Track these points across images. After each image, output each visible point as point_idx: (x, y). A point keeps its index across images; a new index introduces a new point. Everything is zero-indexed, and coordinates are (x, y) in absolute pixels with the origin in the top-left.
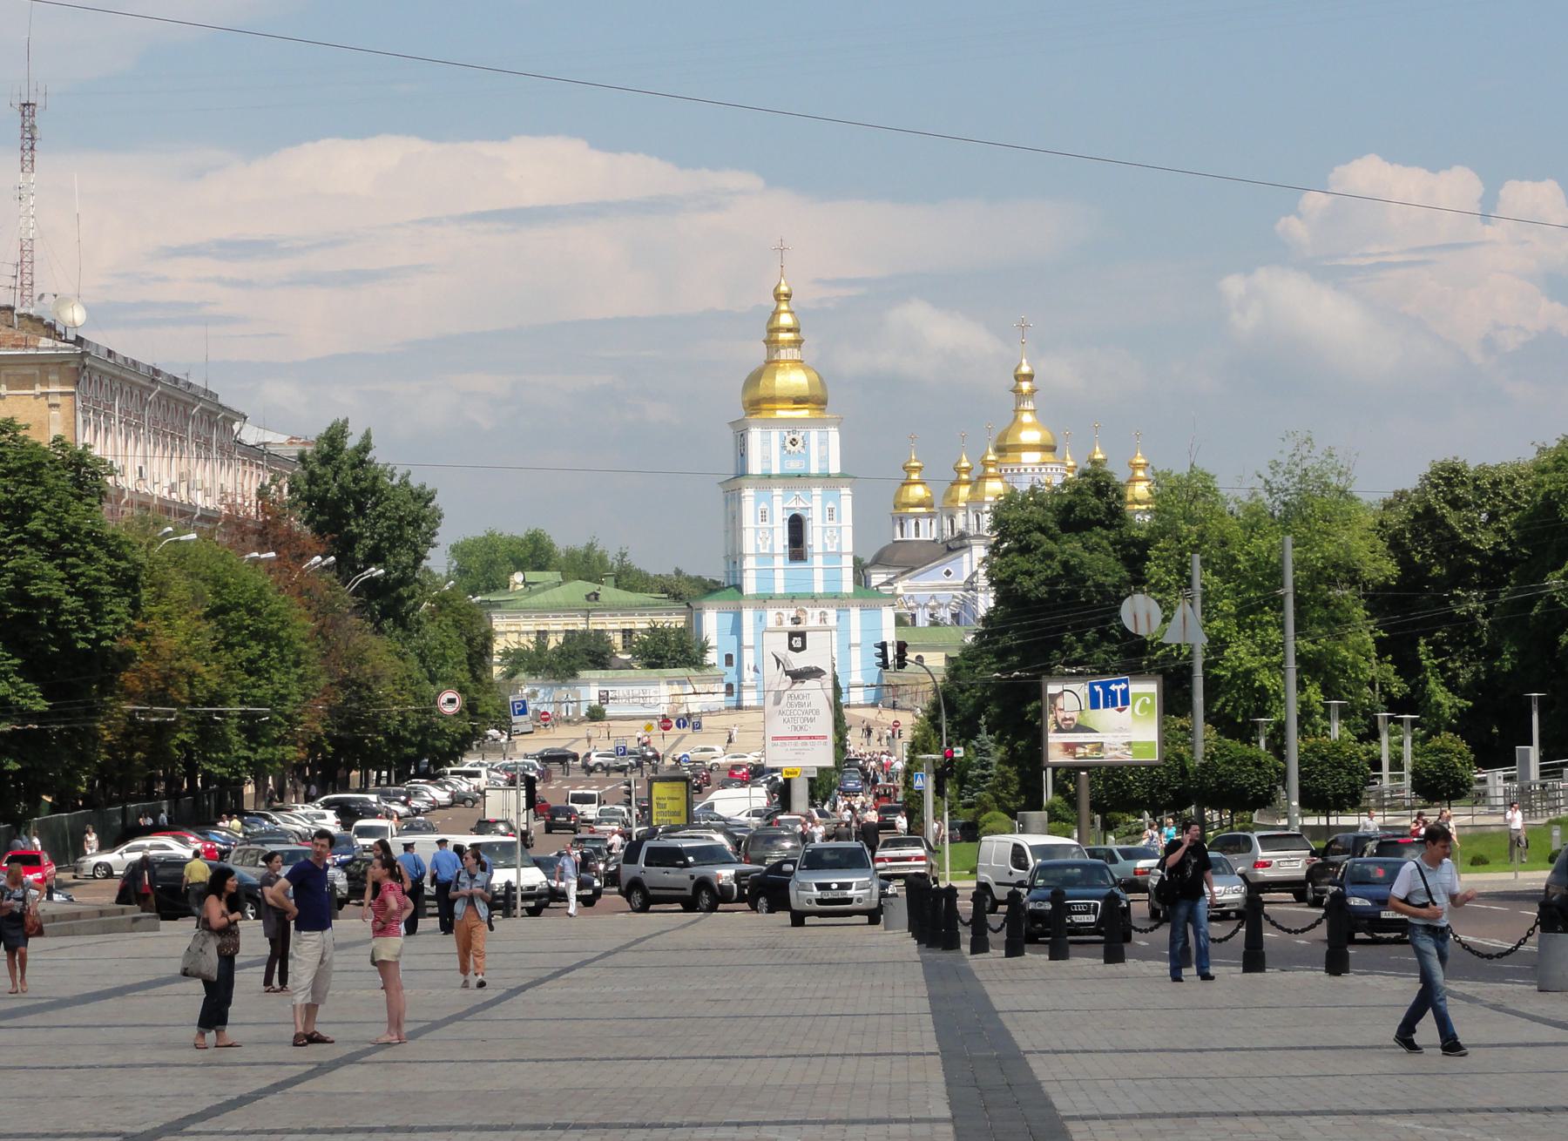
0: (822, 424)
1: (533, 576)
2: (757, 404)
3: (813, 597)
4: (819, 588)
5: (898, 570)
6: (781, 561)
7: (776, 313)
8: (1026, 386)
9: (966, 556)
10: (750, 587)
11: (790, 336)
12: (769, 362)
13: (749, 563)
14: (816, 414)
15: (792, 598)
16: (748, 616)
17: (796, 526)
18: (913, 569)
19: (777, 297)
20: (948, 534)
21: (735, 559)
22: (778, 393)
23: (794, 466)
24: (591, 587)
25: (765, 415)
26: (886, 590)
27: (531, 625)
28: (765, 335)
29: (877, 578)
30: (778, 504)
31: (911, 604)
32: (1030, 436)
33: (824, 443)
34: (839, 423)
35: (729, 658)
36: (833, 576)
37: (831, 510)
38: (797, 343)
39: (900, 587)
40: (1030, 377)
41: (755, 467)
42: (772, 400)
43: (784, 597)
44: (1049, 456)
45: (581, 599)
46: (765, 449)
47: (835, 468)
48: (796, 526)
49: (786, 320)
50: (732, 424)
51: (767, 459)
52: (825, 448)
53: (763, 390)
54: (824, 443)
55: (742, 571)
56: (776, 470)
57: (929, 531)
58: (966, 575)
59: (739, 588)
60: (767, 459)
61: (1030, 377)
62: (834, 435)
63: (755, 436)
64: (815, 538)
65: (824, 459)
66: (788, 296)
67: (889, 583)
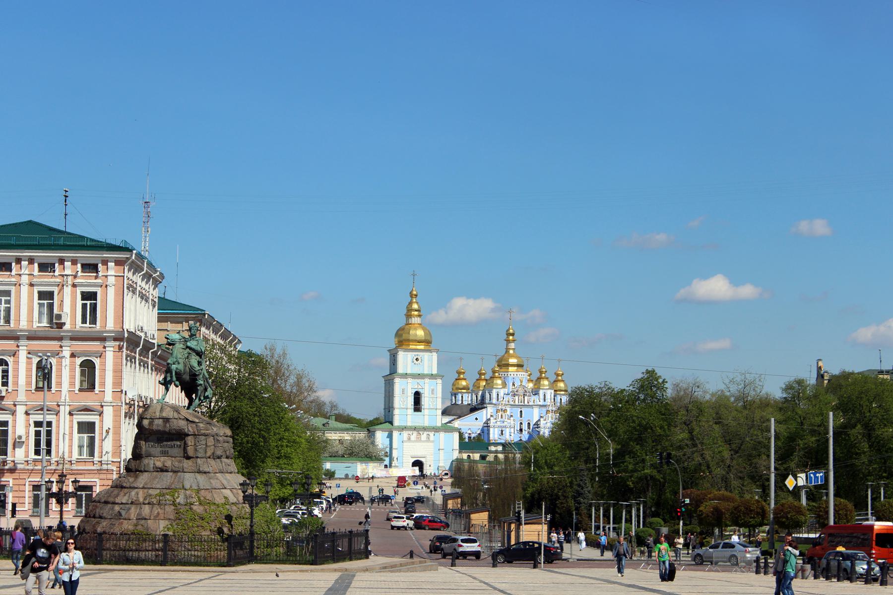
0: (430, 351)
3: (425, 429)
5: (451, 418)
6: (411, 410)
7: (411, 303)
8: (511, 338)
9: (484, 411)
10: (396, 423)
11: (416, 313)
12: (407, 324)
13: (396, 412)
14: (427, 348)
15: (415, 429)
16: (395, 434)
17: (417, 397)
18: (460, 417)
19: (411, 295)
20: (474, 403)
21: (389, 408)
22: (411, 338)
23: (416, 370)
24: (325, 421)
25: (404, 347)
30: (410, 386)
32: (513, 361)
33: (431, 360)
34: (437, 351)
37: (433, 390)
38: (419, 316)
40: (513, 335)
41: (400, 370)
42: (409, 340)
44: (520, 369)
46: (405, 361)
48: (417, 397)
49: (415, 306)
50: (389, 351)
52: (430, 362)
53: (405, 336)
54: (431, 360)
55: (392, 415)
58: (485, 420)
59: (391, 423)
61: (513, 335)
62: (435, 355)
63: (401, 356)
64: (425, 401)
66: (416, 295)
67: (450, 422)
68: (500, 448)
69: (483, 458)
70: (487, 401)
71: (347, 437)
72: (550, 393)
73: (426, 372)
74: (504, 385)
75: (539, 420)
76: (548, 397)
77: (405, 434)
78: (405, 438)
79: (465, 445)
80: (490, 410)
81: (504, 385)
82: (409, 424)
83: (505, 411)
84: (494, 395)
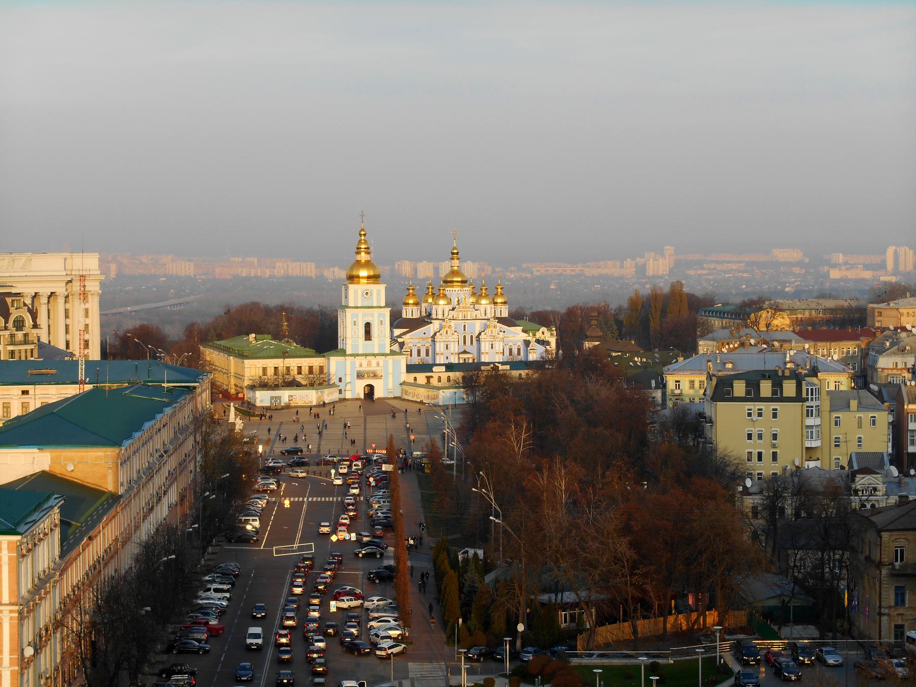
1: (259, 336)
2: (352, 278)
3: (375, 355)
4: (376, 352)
10: (349, 352)
15: (366, 355)
17: (368, 326)
19: (360, 235)
23: (367, 304)
26: (400, 340)
27: (259, 363)
28: (356, 250)
29: (397, 332)
31: (411, 345)
35: (340, 380)
36: (382, 346)
39: (406, 338)
43: (362, 355)
45: (281, 354)
47: (383, 304)
48: (368, 326)
51: (356, 300)
56: (359, 305)
57: (416, 315)
58: (432, 334)
60: (356, 300)
64: (375, 331)
65: (379, 300)
67: (400, 336)
68: (443, 368)
69: (428, 378)
70: (434, 316)
71: (305, 363)
72: (490, 309)
73: (375, 305)
74: (449, 303)
75: (480, 334)
76: (488, 311)
77: (358, 360)
78: (357, 365)
79: (411, 368)
80: (434, 326)
81: (449, 303)
82: (361, 352)
83: (450, 327)
84: (440, 312)
